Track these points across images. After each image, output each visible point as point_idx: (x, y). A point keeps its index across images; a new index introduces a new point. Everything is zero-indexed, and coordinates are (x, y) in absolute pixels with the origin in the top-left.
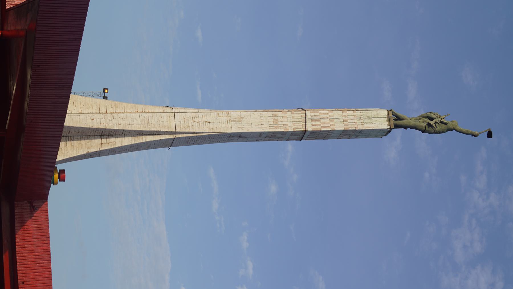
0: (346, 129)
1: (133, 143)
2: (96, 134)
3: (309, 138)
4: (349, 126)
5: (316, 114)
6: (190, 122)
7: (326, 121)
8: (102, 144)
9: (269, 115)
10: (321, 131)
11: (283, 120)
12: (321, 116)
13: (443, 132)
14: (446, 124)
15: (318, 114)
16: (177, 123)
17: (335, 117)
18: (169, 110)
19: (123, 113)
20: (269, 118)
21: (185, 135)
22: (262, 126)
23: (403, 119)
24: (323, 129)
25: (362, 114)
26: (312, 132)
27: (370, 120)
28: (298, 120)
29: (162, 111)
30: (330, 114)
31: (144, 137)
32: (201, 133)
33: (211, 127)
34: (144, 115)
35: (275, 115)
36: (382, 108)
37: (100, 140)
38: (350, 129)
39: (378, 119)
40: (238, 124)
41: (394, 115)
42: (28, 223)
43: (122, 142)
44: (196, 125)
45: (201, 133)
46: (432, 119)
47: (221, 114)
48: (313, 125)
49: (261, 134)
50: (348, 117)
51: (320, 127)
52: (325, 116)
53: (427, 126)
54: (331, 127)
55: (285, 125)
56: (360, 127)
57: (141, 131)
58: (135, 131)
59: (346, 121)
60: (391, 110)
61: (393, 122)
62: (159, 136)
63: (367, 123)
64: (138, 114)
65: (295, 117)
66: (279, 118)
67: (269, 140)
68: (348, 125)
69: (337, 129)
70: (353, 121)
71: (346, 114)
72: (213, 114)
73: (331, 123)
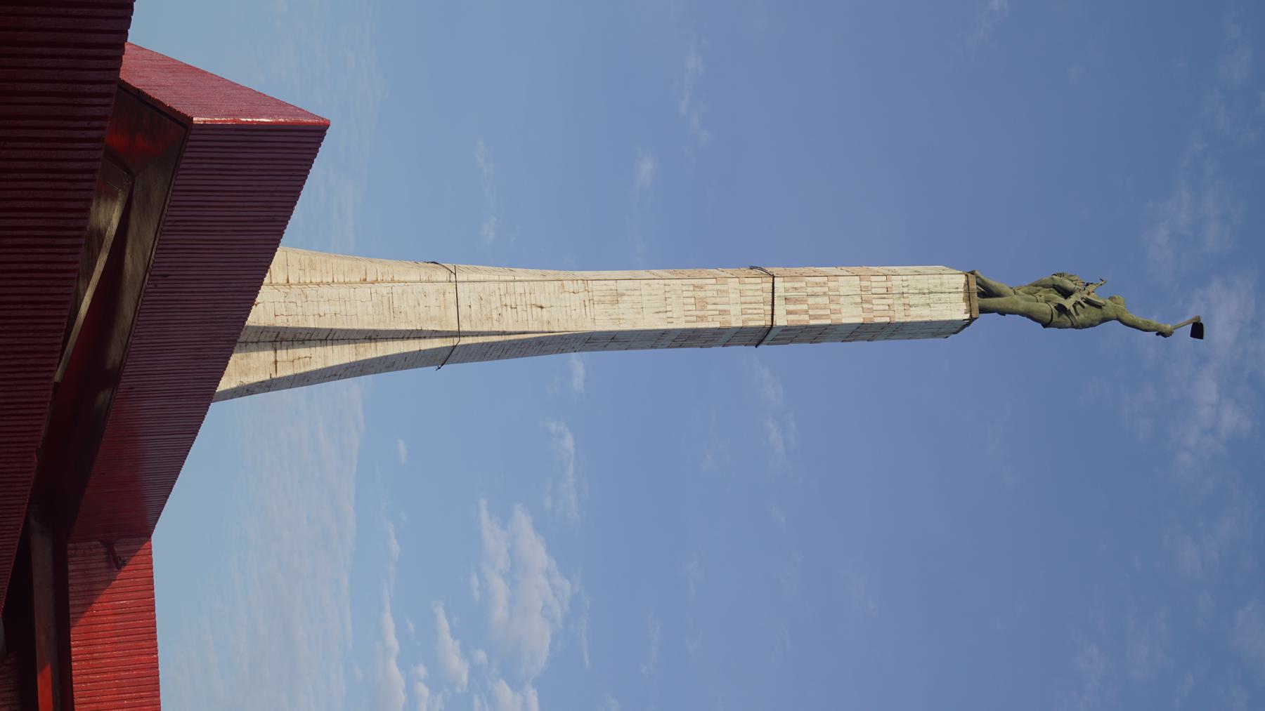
0: (867, 321)
1: (353, 360)
2: (262, 338)
3: (776, 341)
4: (875, 313)
5: (797, 285)
6: (493, 306)
8: (276, 362)
9: (685, 288)
10: (807, 327)
11: (718, 300)
12: (809, 290)
13: (1091, 325)
14: (1099, 306)
15: (803, 284)
16: (463, 310)
17: (843, 291)
18: (442, 275)
19: (328, 283)
20: (686, 294)
21: (480, 340)
22: (669, 314)
23: (999, 295)
24: (812, 322)
25: (905, 284)
26: (786, 329)
27: (924, 299)
28: (753, 299)
29: (424, 278)
30: (830, 284)
31: (379, 344)
32: (520, 333)
34: (383, 289)
35: (700, 287)
36: (952, 264)
37: (272, 352)
38: (878, 320)
39: (938, 294)
41: (981, 284)
42: (102, 598)
43: (326, 357)
44: (508, 313)
45: (520, 333)
46: (1067, 293)
47: (569, 285)
48: (789, 313)
49: (664, 333)
50: (874, 291)
51: (806, 317)
52: (818, 290)
53: (1055, 311)
54: (833, 317)
55: (722, 312)
56: (900, 317)
57: (375, 331)
58: (359, 331)
59: (867, 302)
60: (972, 273)
61: (977, 302)
62: (417, 341)
63: (916, 306)
64: (366, 289)
65: (748, 293)
66: (709, 294)
67: (680, 346)
68: (871, 310)
69: (845, 321)
70: (885, 301)
71: (868, 284)
72: (550, 287)
73: (833, 307)
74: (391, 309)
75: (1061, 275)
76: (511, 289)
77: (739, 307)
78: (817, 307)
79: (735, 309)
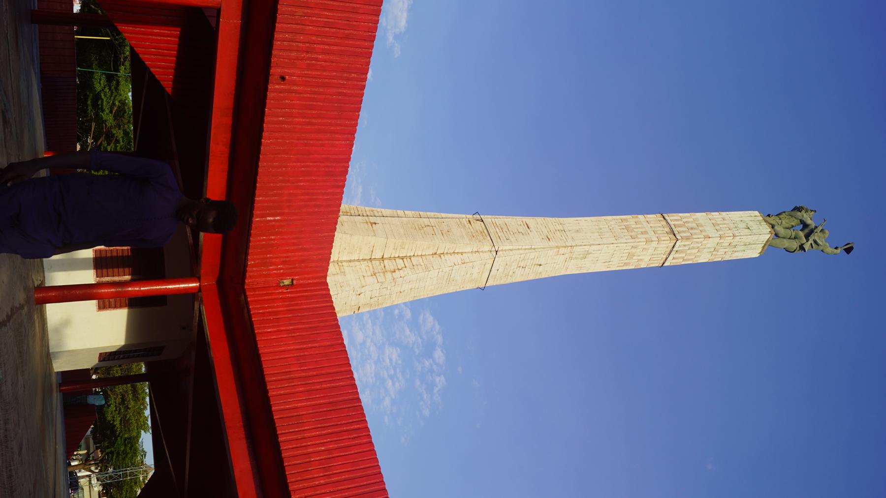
5: (687, 243)
17: (709, 245)
29: (475, 250)
35: (635, 248)
44: (519, 272)
47: (562, 250)
75: (806, 211)
78: (690, 254)
79: (647, 259)
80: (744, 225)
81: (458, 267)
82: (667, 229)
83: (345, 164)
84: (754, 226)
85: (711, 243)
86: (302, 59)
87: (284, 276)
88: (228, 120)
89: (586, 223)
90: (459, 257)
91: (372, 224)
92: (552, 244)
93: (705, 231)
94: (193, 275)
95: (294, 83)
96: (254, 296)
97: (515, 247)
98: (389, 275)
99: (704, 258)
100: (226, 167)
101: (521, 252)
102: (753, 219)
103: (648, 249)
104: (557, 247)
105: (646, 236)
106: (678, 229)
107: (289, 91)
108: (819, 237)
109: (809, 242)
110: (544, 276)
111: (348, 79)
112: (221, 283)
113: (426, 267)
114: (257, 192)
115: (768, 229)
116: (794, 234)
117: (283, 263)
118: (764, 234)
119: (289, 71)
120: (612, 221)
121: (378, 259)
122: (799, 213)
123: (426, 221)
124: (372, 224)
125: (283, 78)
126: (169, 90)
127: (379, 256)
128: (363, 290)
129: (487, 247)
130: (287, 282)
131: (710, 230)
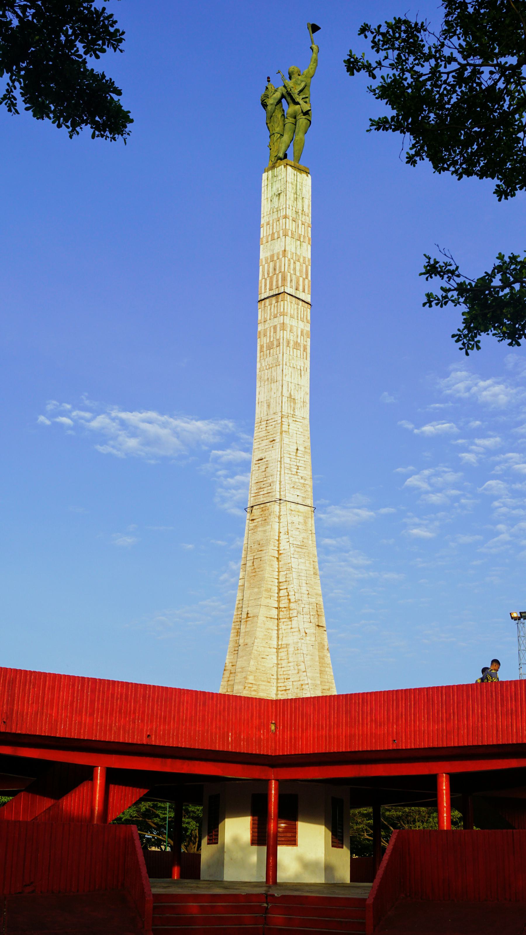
6: (297, 480)
7: (298, 268)
15: (289, 274)
16: (299, 500)
17: (293, 250)
20: (291, 353)
22: (302, 369)
24: (310, 278)
29: (277, 520)
33: (303, 449)
35: (288, 343)
40: (299, 406)
44: (301, 473)
50: (294, 230)
51: (306, 281)
54: (307, 263)
59: (300, 238)
63: (303, 207)
70: (300, 226)
72: (286, 440)
73: (301, 260)
74: (301, 547)
75: (267, 96)
76: (288, 466)
77: (300, 322)
78: (301, 271)
79: (301, 325)
80: (276, 199)
81: (291, 539)
82: (274, 300)
83: (199, 693)
84: (277, 186)
85: (291, 246)
86: (138, 725)
87: (269, 729)
88: (169, 761)
89: (262, 393)
90: (283, 536)
91: (248, 617)
92: (278, 439)
93: (278, 254)
94: (267, 782)
95: (151, 729)
96: (279, 750)
97: (278, 479)
98: (292, 605)
99: (306, 251)
100: (197, 762)
101: (282, 473)
102: (269, 188)
103: (291, 326)
104: (281, 433)
105: (278, 329)
106: (274, 287)
107: (156, 732)
108: (296, 83)
109: (301, 102)
110: (308, 444)
111: (149, 697)
112: (273, 766)
113: (288, 569)
114: (213, 749)
115: (281, 169)
116: (292, 120)
117: (260, 730)
118: (286, 173)
119: (145, 733)
120: (262, 363)
121: (279, 612)
122: (269, 108)
123: (249, 564)
124: (248, 617)
125: (149, 736)
126: (145, 791)
127: (275, 612)
128: (302, 631)
129: (276, 508)
130: (273, 727)
131: (278, 247)
